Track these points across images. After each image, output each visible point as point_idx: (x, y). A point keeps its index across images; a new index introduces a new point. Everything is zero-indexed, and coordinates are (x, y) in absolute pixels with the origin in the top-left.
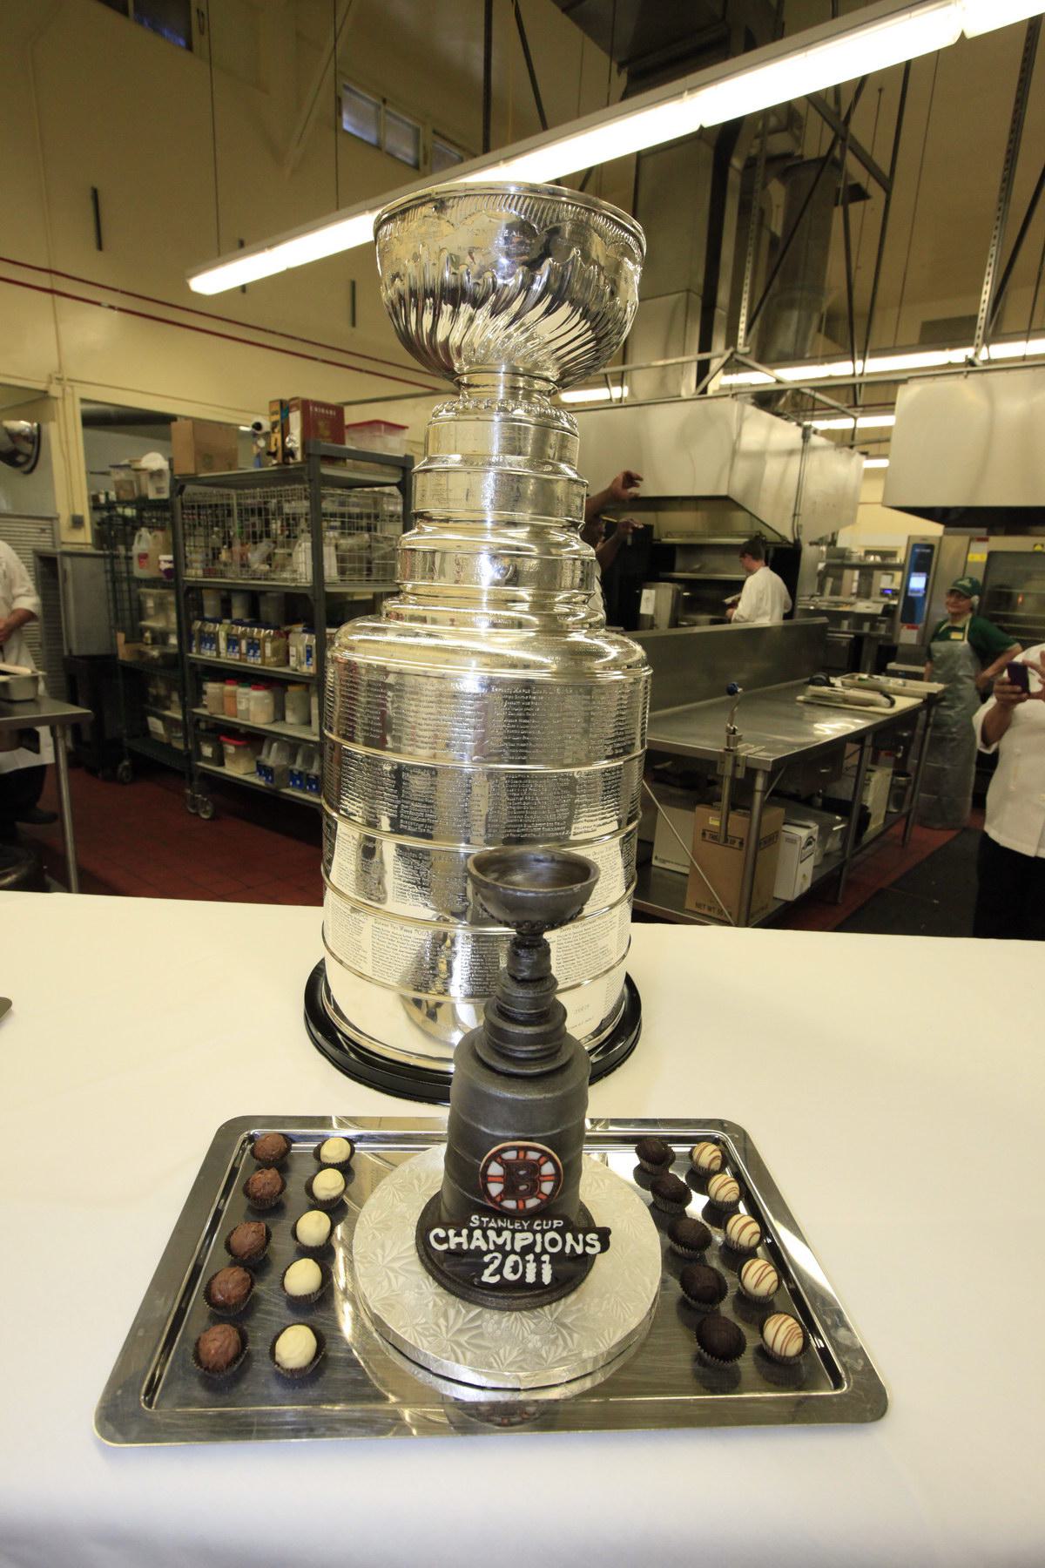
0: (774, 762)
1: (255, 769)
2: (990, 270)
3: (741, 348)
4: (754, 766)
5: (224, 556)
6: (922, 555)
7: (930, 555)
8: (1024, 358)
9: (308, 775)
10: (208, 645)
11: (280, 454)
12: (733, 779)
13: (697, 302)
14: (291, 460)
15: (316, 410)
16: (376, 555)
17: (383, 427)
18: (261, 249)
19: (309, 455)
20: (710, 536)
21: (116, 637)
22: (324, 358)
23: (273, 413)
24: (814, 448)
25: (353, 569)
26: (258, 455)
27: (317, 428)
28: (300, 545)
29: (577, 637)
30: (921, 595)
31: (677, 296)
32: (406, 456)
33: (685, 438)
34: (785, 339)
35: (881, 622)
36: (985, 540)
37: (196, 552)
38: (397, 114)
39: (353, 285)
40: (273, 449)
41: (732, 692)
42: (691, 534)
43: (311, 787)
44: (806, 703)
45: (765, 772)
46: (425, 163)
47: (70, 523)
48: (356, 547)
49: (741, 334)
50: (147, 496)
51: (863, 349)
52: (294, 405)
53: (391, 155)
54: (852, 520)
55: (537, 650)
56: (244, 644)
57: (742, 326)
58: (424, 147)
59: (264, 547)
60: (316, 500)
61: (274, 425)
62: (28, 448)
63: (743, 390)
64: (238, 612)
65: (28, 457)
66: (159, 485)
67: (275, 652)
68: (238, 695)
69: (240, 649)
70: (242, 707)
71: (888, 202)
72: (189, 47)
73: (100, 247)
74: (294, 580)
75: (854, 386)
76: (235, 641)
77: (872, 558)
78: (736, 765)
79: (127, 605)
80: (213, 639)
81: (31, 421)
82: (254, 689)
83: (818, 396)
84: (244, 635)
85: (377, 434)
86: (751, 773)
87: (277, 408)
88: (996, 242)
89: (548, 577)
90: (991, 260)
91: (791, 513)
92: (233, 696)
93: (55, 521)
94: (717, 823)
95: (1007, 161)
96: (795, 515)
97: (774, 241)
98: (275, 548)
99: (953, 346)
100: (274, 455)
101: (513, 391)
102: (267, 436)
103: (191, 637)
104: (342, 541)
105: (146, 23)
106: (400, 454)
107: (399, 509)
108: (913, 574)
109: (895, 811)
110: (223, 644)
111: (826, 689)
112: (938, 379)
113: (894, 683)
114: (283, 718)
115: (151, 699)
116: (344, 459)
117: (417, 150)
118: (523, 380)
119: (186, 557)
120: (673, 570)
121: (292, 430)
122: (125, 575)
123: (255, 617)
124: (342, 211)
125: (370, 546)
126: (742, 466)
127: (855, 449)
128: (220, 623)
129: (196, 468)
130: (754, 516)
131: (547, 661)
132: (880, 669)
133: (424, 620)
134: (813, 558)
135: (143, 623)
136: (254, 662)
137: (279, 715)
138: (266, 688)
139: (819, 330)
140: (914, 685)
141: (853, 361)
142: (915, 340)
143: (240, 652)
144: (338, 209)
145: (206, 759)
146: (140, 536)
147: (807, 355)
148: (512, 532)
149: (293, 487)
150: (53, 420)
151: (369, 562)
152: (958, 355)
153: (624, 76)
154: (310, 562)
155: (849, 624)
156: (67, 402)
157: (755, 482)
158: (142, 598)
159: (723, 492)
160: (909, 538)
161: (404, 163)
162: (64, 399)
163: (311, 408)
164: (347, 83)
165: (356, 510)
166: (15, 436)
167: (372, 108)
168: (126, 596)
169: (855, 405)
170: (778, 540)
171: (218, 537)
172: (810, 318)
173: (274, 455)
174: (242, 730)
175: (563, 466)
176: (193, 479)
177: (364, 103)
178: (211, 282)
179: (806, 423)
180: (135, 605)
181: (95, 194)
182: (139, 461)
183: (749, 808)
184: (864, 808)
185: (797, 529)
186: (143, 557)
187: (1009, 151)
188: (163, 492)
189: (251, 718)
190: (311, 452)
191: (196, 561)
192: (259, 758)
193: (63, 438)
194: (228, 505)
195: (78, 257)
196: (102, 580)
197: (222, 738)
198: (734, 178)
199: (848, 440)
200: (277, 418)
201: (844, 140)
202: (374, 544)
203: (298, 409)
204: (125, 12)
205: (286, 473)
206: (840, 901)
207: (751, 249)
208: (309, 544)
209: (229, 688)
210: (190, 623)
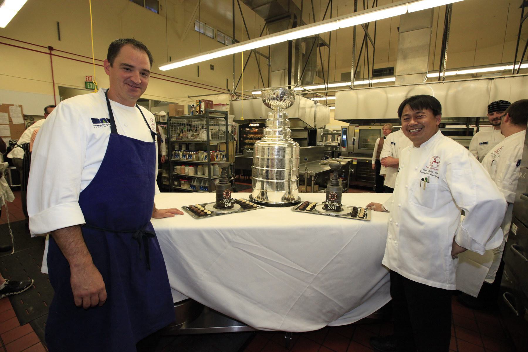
0: (316, 174)
1: (189, 186)
2: (352, 68)
3: (299, 84)
4: (311, 175)
5: (181, 135)
7: (347, 130)
8: (363, 85)
9: (205, 186)
10: (177, 157)
11: (199, 112)
12: (307, 178)
13: (287, 72)
14: (202, 113)
16: (219, 134)
17: (221, 105)
18: (180, 61)
20: (294, 127)
22: (191, 85)
23: (197, 103)
24: (318, 106)
25: (215, 137)
26: (192, 112)
28: (203, 132)
29: (290, 142)
30: (345, 140)
32: (226, 111)
34: (308, 79)
35: (338, 147)
36: (358, 127)
37: (174, 134)
38: (209, 27)
39: (198, 66)
40: (197, 111)
41: (306, 160)
43: (206, 190)
44: (321, 164)
45: (314, 176)
46: (216, 37)
48: (215, 132)
49: (299, 80)
50: (160, 121)
51: (327, 82)
53: (207, 36)
54: (329, 123)
55: (287, 143)
56: (187, 156)
57: (299, 79)
58: (215, 34)
59: (191, 133)
60: (208, 122)
61: (197, 105)
63: (300, 93)
64: (184, 148)
66: (164, 119)
67: (196, 157)
68: (185, 168)
69: (186, 157)
70: (187, 171)
72: (158, 13)
74: (202, 140)
75: (326, 92)
76: (185, 155)
77: (334, 132)
78: (307, 175)
80: (179, 155)
82: (191, 167)
83: (317, 94)
84: (187, 154)
85: (220, 107)
86: (311, 176)
87: (199, 102)
88: (352, 63)
89: (286, 134)
90: (352, 66)
91: (314, 121)
92: (184, 169)
94: (304, 189)
95: (353, 47)
96: (314, 122)
97: (303, 55)
99: (348, 82)
100: (197, 112)
101: (280, 110)
103: (172, 155)
104: (212, 131)
105: (148, 8)
106: (225, 110)
107: (224, 123)
108: (343, 135)
109: (344, 189)
110: (181, 156)
111: (325, 161)
112: (344, 91)
113: (340, 160)
114: (197, 174)
116: (213, 112)
117: (214, 35)
118: (281, 109)
119: (172, 136)
121: (202, 107)
123: (187, 149)
125: (218, 132)
126: (300, 111)
127: (327, 106)
128: (180, 151)
131: (286, 144)
132: (338, 158)
133: (268, 140)
134: (320, 132)
136: (190, 160)
137: (196, 173)
138: (193, 166)
139: (316, 75)
140: (345, 160)
142: (340, 80)
143: (186, 158)
145: (176, 185)
147: (313, 83)
148: (280, 128)
149: (202, 119)
151: (218, 136)
152: (349, 84)
153: (266, 22)
154: (206, 136)
155: (330, 148)
157: (304, 114)
159: (297, 117)
160: (341, 127)
161: (211, 38)
165: (213, 124)
169: (327, 95)
170: (311, 128)
171: (179, 131)
172: (314, 73)
173: (197, 112)
174: (186, 177)
175: (287, 119)
179: (315, 99)
182: (159, 113)
183: (311, 186)
187: (353, 45)
188: (165, 120)
189: (189, 174)
190: (207, 111)
191: (174, 137)
192: (191, 184)
197: (180, 180)
198: (294, 45)
199: (326, 103)
200: (198, 104)
201: (318, 38)
202: (219, 131)
203: (204, 102)
204: (143, 6)
205: (200, 116)
207: (299, 62)
209: (183, 167)
210: (172, 152)
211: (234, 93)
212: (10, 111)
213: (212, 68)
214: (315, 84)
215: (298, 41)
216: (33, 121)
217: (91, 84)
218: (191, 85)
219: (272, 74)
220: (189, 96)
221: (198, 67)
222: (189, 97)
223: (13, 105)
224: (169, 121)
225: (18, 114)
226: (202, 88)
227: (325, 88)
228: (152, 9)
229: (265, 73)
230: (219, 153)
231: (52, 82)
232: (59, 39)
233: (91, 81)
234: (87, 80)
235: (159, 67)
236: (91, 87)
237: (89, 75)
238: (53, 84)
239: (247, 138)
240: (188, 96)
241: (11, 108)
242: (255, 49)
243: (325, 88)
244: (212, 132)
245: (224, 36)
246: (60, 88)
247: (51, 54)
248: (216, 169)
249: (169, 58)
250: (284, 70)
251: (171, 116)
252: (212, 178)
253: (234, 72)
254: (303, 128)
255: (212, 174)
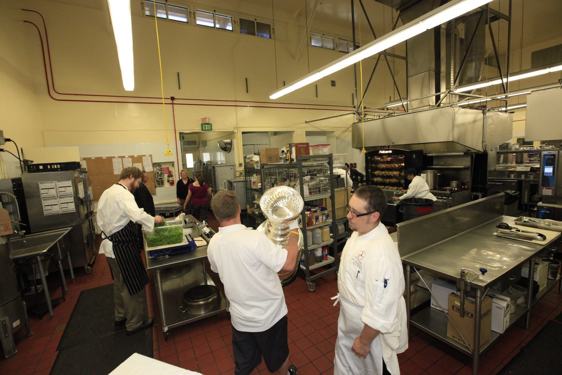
6: (549, 159)
11: (289, 160)
13: (434, 73)
14: (293, 162)
15: (300, 146)
19: (298, 160)
20: (447, 152)
21: (247, 206)
23: (288, 148)
27: (301, 151)
30: (551, 175)
31: (425, 73)
33: (433, 121)
34: (471, 73)
40: (288, 159)
42: (440, 152)
46: (336, 47)
47: (239, 166)
51: (506, 74)
52: (293, 145)
53: (326, 48)
58: (336, 43)
61: (288, 151)
62: (229, 146)
65: (229, 148)
71: (510, 24)
73: (247, 92)
79: (250, 197)
81: (230, 139)
87: (288, 146)
93: (235, 166)
96: (483, 142)
98: (291, 183)
100: (288, 160)
102: (286, 154)
108: (546, 167)
112: (546, 91)
115: (256, 224)
116: (310, 159)
117: (334, 45)
119: (265, 187)
120: (433, 165)
122: (249, 188)
124: (310, 73)
127: (507, 112)
129: (267, 161)
130: (465, 146)
135: (254, 201)
141: (502, 79)
144: (309, 73)
146: (254, 176)
150: (235, 139)
151: (319, 188)
153: (399, 12)
156: (238, 133)
158: (254, 194)
159: (451, 140)
162: (238, 132)
163: (298, 146)
164: (312, 33)
166: (226, 144)
167: (320, 37)
168: (250, 194)
173: (288, 160)
176: (267, 165)
177: (318, 37)
178: (274, 96)
180: (252, 196)
181: (246, 79)
184: (535, 283)
185: (485, 147)
186: (254, 183)
190: (299, 159)
193: (237, 143)
194: (276, 173)
195: (243, 96)
196: (243, 189)
198: (443, 32)
200: (288, 149)
201: (487, 10)
202: (320, 182)
206: (527, 328)
208: (299, 186)
211: (357, 112)
212: (143, 161)
213: (333, 84)
214: (484, 80)
215: (449, 23)
216: (161, 167)
217: (206, 126)
218: (308, 109)
219: (409, 79)
220: (307, 121)
221: (316, 86)
222: (306, 122)
223: (145, 156)
224: (261, 168)
225: (148, 163)
226: (321, 109)
227: (503, 83)
228: (265, 35)
229: (401, 77)
230: (321, 212)
231: (174, 129)
232: (180, 88)
233: (206, 123)
234: (203, 122)
235: (270, 96)
236: (207, 128)
237: (204, 117)
238: (174, 131)
239: (377, 169)
240: (306, 121)
241: (144, 158)
242: (385, 51)
243: (503, 83)
244: (310, 186)
245: (348, 43)
246: (180, 133)
247: (173, 104)
248: (317, 236)
249: (283, 84)
250: (428, 72)
251: (263, 162)
252: (309, 250)
253: (356, 87)
254: (462, 153)
255: (310, 241)
